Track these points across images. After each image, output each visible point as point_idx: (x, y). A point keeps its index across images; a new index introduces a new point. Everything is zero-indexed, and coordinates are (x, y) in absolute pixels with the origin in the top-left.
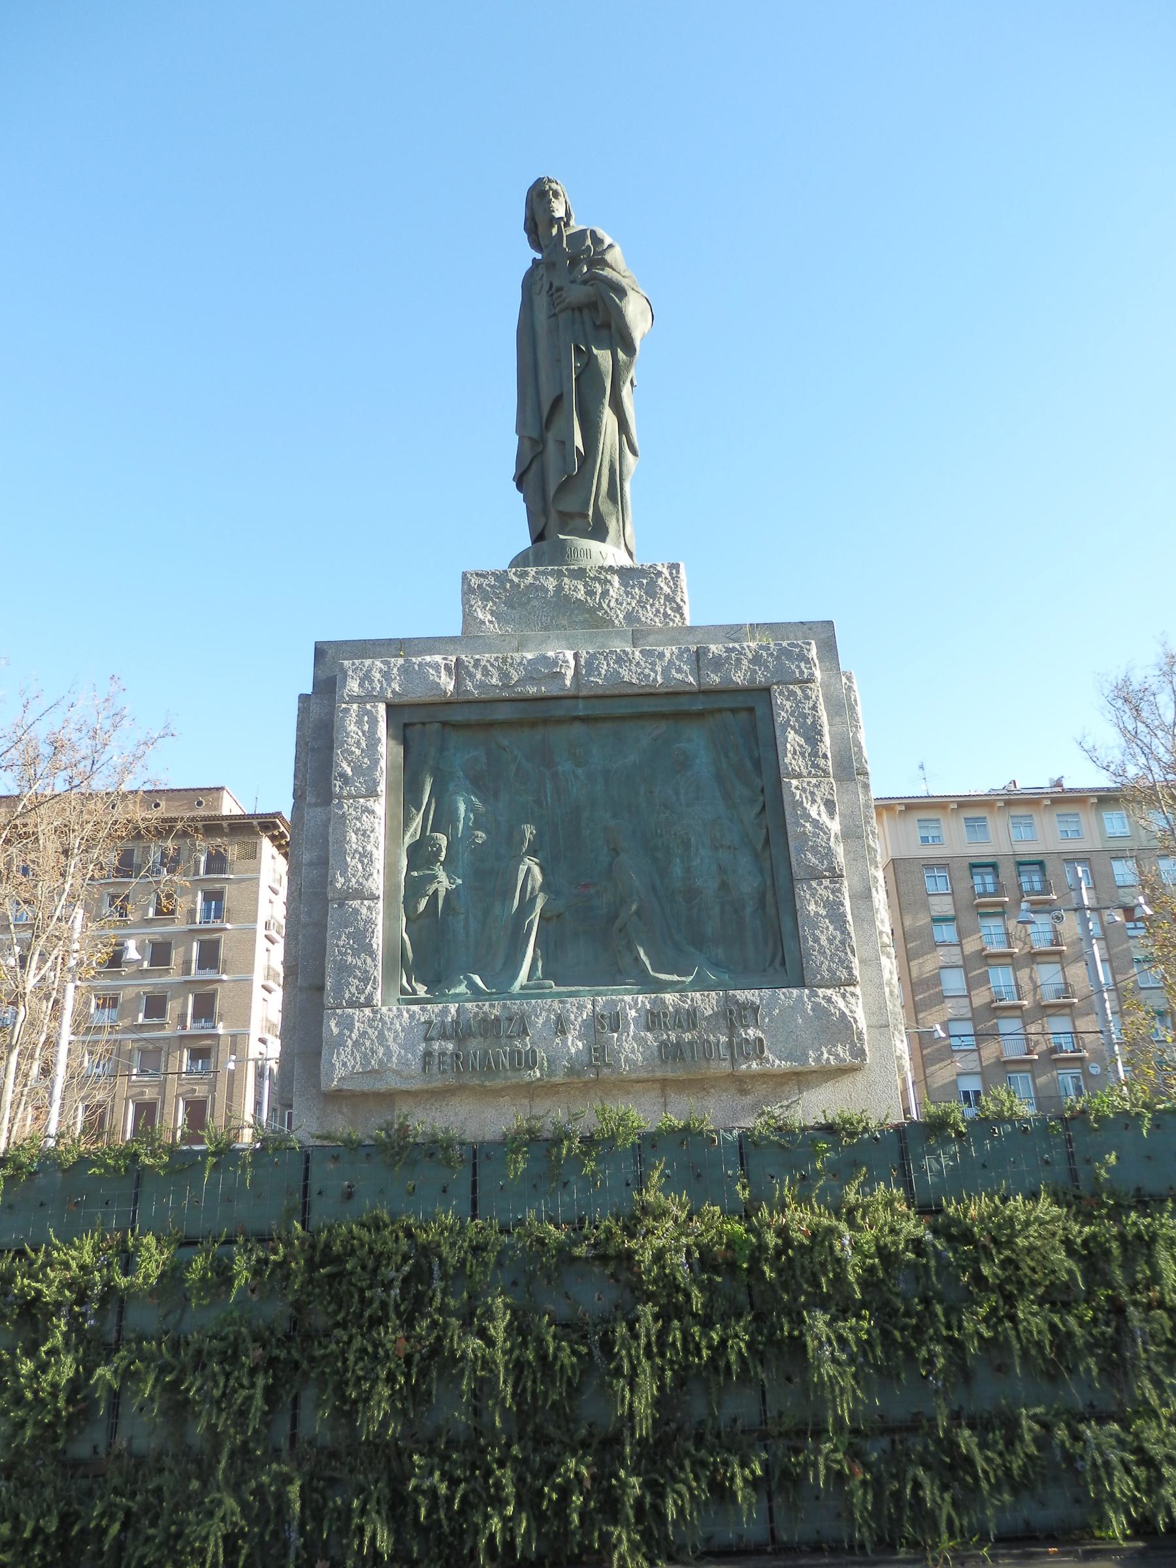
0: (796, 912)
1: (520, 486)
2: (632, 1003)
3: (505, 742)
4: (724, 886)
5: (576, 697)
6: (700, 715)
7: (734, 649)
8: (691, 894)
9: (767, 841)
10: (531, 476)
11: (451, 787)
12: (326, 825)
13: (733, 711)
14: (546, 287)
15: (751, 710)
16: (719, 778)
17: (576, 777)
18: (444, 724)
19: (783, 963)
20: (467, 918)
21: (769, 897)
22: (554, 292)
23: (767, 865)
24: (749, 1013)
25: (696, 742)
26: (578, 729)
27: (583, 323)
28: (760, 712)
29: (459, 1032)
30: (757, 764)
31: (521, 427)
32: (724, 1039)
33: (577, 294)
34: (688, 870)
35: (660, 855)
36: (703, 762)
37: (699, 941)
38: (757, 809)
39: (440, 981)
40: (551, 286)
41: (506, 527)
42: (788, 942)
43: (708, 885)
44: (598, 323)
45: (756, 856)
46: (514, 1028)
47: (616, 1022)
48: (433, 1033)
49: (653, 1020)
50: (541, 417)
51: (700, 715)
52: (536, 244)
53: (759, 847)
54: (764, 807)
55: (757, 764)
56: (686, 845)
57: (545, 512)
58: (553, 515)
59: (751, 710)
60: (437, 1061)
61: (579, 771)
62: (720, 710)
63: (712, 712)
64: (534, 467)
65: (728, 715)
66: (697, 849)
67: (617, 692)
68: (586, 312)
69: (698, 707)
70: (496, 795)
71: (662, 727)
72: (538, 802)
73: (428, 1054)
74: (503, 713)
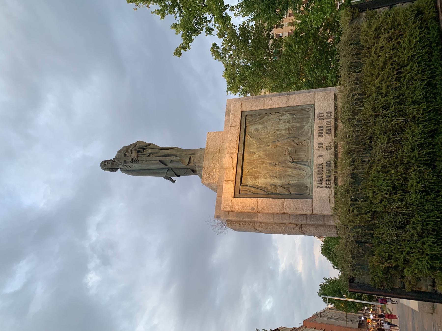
2: (317, 140)
3: (247, 171)
4: (288, 122)
6: (246, 127)
8: (289, 129)
9: (278, 113)
11: (257, 184)
12: (263, 213)
13: (246, 119)
14: (130, 164)
15: (246, 116)
16: (261, 123)
18: (240, 185)
19: (308, 109)
21: (292, 112)
22: (133, 161)
23: (284, 113)
25: (251, 129)
28: (247, 113)
30: (259, 115)
32: (326, 120)
33: (134, 155)
34: (284, 130)
35: (279, 136)
37: (302, 127)
40: (131, 162)
45: (282, 115)
46: (321, 167)
48: (321, 186)
49: (321, 135)
51: (246, 127)
52: (116, 169)
55: (259, 115)
56: (278, 130)
61: (256, 154)
64: (175, 171)
70: (260, 173)
71: (248, 136)
72: (263, 163)
73: (326, 187)
74: (239, 170)
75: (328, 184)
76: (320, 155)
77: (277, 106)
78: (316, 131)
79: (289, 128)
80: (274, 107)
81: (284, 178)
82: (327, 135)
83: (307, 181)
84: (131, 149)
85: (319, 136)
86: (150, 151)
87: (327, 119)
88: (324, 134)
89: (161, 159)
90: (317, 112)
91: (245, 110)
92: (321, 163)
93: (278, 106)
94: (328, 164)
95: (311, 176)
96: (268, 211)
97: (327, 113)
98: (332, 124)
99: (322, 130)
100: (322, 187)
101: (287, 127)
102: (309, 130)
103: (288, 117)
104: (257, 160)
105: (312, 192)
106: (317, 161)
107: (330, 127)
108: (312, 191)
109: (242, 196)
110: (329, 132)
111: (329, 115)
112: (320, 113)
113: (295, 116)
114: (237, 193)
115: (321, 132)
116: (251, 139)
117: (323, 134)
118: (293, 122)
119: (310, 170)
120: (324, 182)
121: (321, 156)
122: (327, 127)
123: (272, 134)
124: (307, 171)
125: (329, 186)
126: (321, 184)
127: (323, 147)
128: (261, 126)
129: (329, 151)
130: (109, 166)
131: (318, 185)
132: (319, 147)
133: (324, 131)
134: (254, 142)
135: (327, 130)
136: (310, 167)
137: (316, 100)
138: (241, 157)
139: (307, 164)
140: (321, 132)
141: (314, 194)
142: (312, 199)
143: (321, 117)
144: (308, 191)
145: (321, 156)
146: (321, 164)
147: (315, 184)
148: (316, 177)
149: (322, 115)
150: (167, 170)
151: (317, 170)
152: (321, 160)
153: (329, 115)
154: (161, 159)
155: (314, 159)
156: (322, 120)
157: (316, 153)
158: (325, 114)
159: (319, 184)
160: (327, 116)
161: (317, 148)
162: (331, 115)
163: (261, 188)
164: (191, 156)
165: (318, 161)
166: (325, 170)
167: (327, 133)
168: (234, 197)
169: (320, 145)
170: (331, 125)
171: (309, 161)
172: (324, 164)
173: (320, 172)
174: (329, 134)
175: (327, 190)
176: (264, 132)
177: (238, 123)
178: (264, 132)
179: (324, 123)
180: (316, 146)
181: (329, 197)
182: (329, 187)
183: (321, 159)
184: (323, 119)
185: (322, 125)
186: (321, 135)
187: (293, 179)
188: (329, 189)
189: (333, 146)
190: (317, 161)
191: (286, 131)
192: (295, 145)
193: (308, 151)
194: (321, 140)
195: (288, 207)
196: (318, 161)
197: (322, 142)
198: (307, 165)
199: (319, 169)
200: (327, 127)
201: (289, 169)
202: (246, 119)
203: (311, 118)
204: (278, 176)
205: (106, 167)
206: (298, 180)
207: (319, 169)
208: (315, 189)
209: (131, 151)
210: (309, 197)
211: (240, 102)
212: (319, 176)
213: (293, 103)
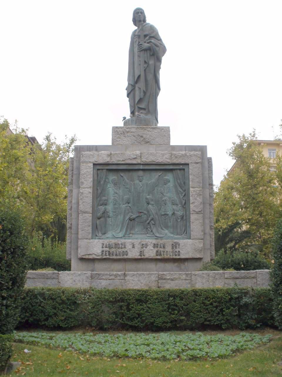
1: (128, 96)
10: (132, 94)
14: (137, 42)
15: (184, 169)
16: (175, 186)
17: (139, 185)
18: (107, 169)
22: (140, 45)
24: (177, 245)
25: (169, 176)
26: (141, 173)
27: (147, 54)
28: (186, 170)
29: (110, 247)
30: (184, 183)
31: (129, 80)
36: (171, 184)
37: (167, 227)
38: (183, 194)
39: (105, 234)
40: (139, 43)
41: (123, 109)
43: (170, 213)
44: (151, 54)
46: (123, 247)
47: (146, 245)
50: (135, 80)
53: (183, 205)
54: (185, 195)
57: (134, 107)
58: (136, 108)
59: (184, 169)
62: (177, 169)
65: (178, 171)
67: (151, 163)
68: (148, 51)
69: (171, 167)
70: (119, 188)
73: (103, 251)
75: (106, 253)
77: (191, 201)
79: (168, 215)
80: (191, 198)
83: (109, 234)
84: (152, 41)
86: (151, 62)
89: (142, 78)
90: (182, 242)
91: (190, 168)
92: (126, 247)
93: (191, 202)
95: (114, 237)
96: (80, 198)
97: (179, 251)
98: (166, 256)
100: (103, 247)
101: (168, 213)
102: (163, 234)
103: (180, 213)
104: (134, 184)
106: (128, 242)
108: (99, 239)
109: (95, 171)
111: (177, 254)
112: (179, 245)
113: (179, 220)
116: (157, 176)
117: (156, 249)
118: (173, 219)
119: (120, 236)
120: (107, 249)
121: (133, 247)
123: (161, 198)
124: (120, 234)
127: (142, 248)
128: (172, 185)
130: (139, 17)
132: (143, 244)
134: (153, 180)
135: (161, 251)
136: (124, 236)
137: (194, 241)
139: (128, 233)
140: (159, 246)
141: (97, 240)
142: (92, 239)
143: (175, 245)
144: (100, 235)
145: (133, 247)
146: (125, 247)
147: (106, 242)
148: (113, 241)
149: (177, 247)
150: (133, 84)
151: (120, 243)
152: (129, 247)
154: (142, 78)
155: (130, 240)
157: (137, 242)
158: (177, 250)
159: (106, 245)
160: (176, 252)
161: (142, 243)
163: (104, 190)
164: (147, 110)
165: (128, 244)
168: (94, 164)
170: (165, 256)
171: (131, 235)
174: (156, 253)
175: (99, 252)
176: (164, 190)
177: (175, 161)
178: (164, 190)
179: (169, 249)
181: (94, 254)
182: (102, 253)
183: (130, 247)
184: (173, 248)
186: (155, 246)
188: (101, 254)
189: (143, 257)
192: (148, 222)
193: (141, 234)
195: (84, 217)
196: (128, 244)
197: (148, 247)
198: (126, 233)
199: (121, 246)
201: (122, 216)
203: (176, 236)
204: (117, 206)
205: (136, 15)
207: (121, 246)
208: (101, 241)
209: (150, 42)
210: (94, 235)
211: (200, 161)
213: (193, 217)
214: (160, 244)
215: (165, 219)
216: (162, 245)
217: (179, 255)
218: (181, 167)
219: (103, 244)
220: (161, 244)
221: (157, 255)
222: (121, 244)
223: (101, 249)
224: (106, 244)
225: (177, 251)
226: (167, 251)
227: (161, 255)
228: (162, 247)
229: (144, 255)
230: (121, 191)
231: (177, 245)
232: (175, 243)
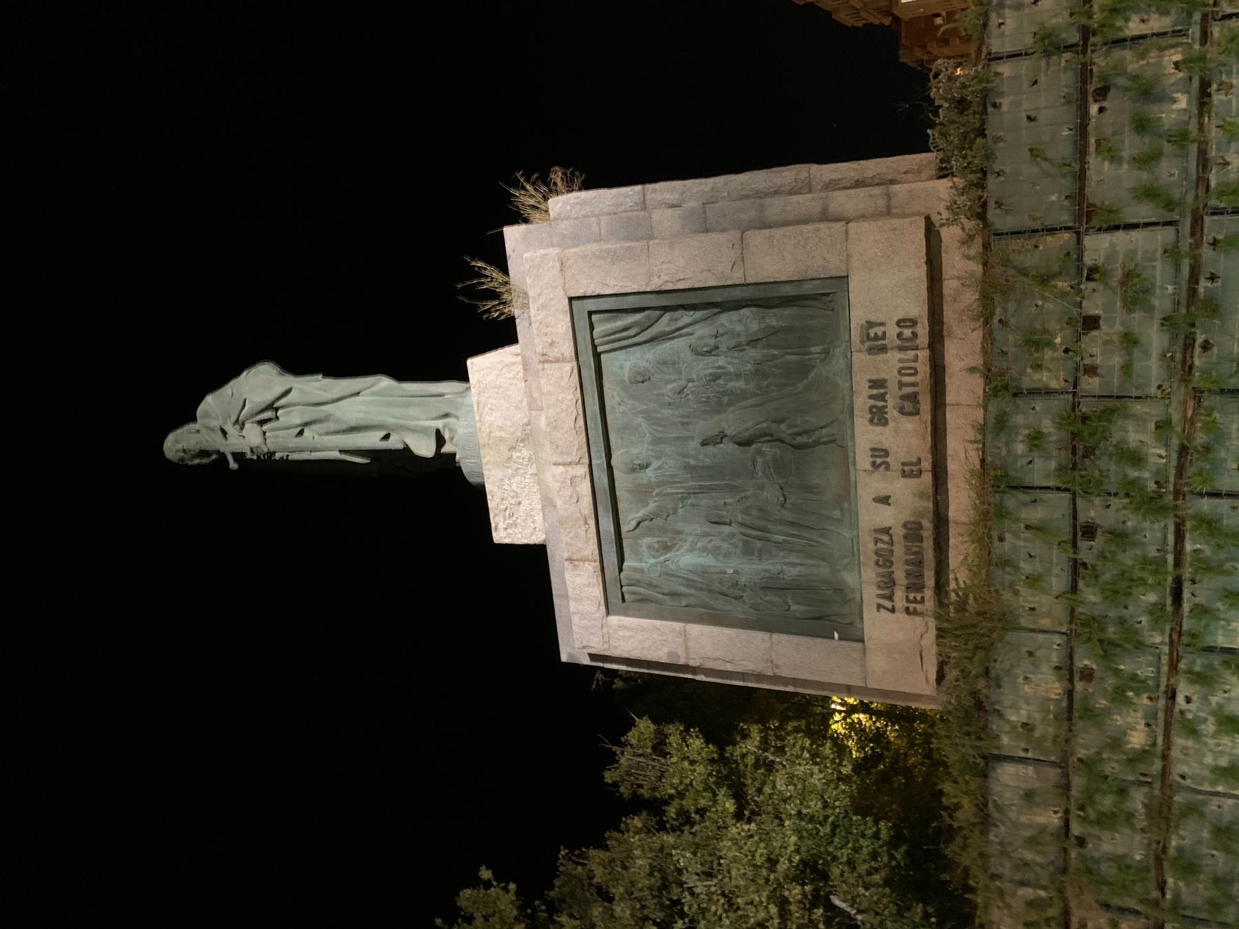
0: (775, 282)
4: (753, 342)
5: (590, 465)
6: (597, 356)
7: (538, 329)
17: (659, 468)
20: (786, 564)
24: (872, 332)
29: (889, 583)
35: (726, 399)
37: (804, 369)
42: (807, 289)
46: (886, 538)
49: (878, 416)
60: (914, 605)
63: (594, 347)
66: (719, 368)
70: (679, 533)
73: (907, 610)
74: (607, 524)
75: (915, 601)
76: (884, 493)
78: (862, 402)
81: (760, 555)
82: (904, 419)
85: (871, 421)
87: (901, 349)
88: (892, 413)
90: (858, 317)
94: (913, 532)
97: (899, 323)
99: (882, 397)
100: (893, 610)
104: (659, 484)
105: (862, 619)
106: (872, 516)
107: (914, 384)
110: (910, 405)
111: (907, 333)
112: (871, 324)
114: (615, 599)
115: (881, 404)
120: (899, 594)
122: (901, 385)
125: (919, 607)
126: (890, 598)
127: (888, 467)
129: (913, 482)
131: (882, 601)
132: (873, 464)
133: (891, 402)
135: (902, 398)
138: (605, 479)
140: (881, 404)
142: (862, 641)
145: (884, 500)
146: (887, 531)
147: (870, 595)
148: (870, 574)
149: (879, 330)
152: (886, 516)
153: (907, 333)
156: (882, 357)
157: (868, 485)
158: (892, 330)
160: (899, 335)
161: (868, 466)
162: (915, 335)
166: (899, 550)
167: (902, 411)
169: (880, 455)
172: (899, 532)
173: (884, 560)
174: (911, 414)
177: (567, 348)
180: (863, 460)
182: (916, 613)
184: (883, 349)
185: (883, 376)
187: (793, 559)
188: (918, 619)
189: (927, 465)
190: (872, 516)
191: (747, 380)
194: (884, 436)
197: (886, 446)
199: (880, 545)
200: (901, 385)
202: (592, 328)
206: (812, 566)
208: (869, 614)
210: (854, 636)
212: (881, 570)
214: (872, 402)
215: (774, 375)
216: (875, 392)
217: (913, 322)
218: (583, 324)
219: (879, 607)
220: (871, 397)
221: (917, 412)
222: (876, 543)
223: (900, 615)
224: (879, 596)
225: (897, 330)
226: (899, 372)
227: (913, 398)
228: (882, 391)
229: (919, 459)
230: (688, 529)
231: (872, 332)
232: (862, 342)
